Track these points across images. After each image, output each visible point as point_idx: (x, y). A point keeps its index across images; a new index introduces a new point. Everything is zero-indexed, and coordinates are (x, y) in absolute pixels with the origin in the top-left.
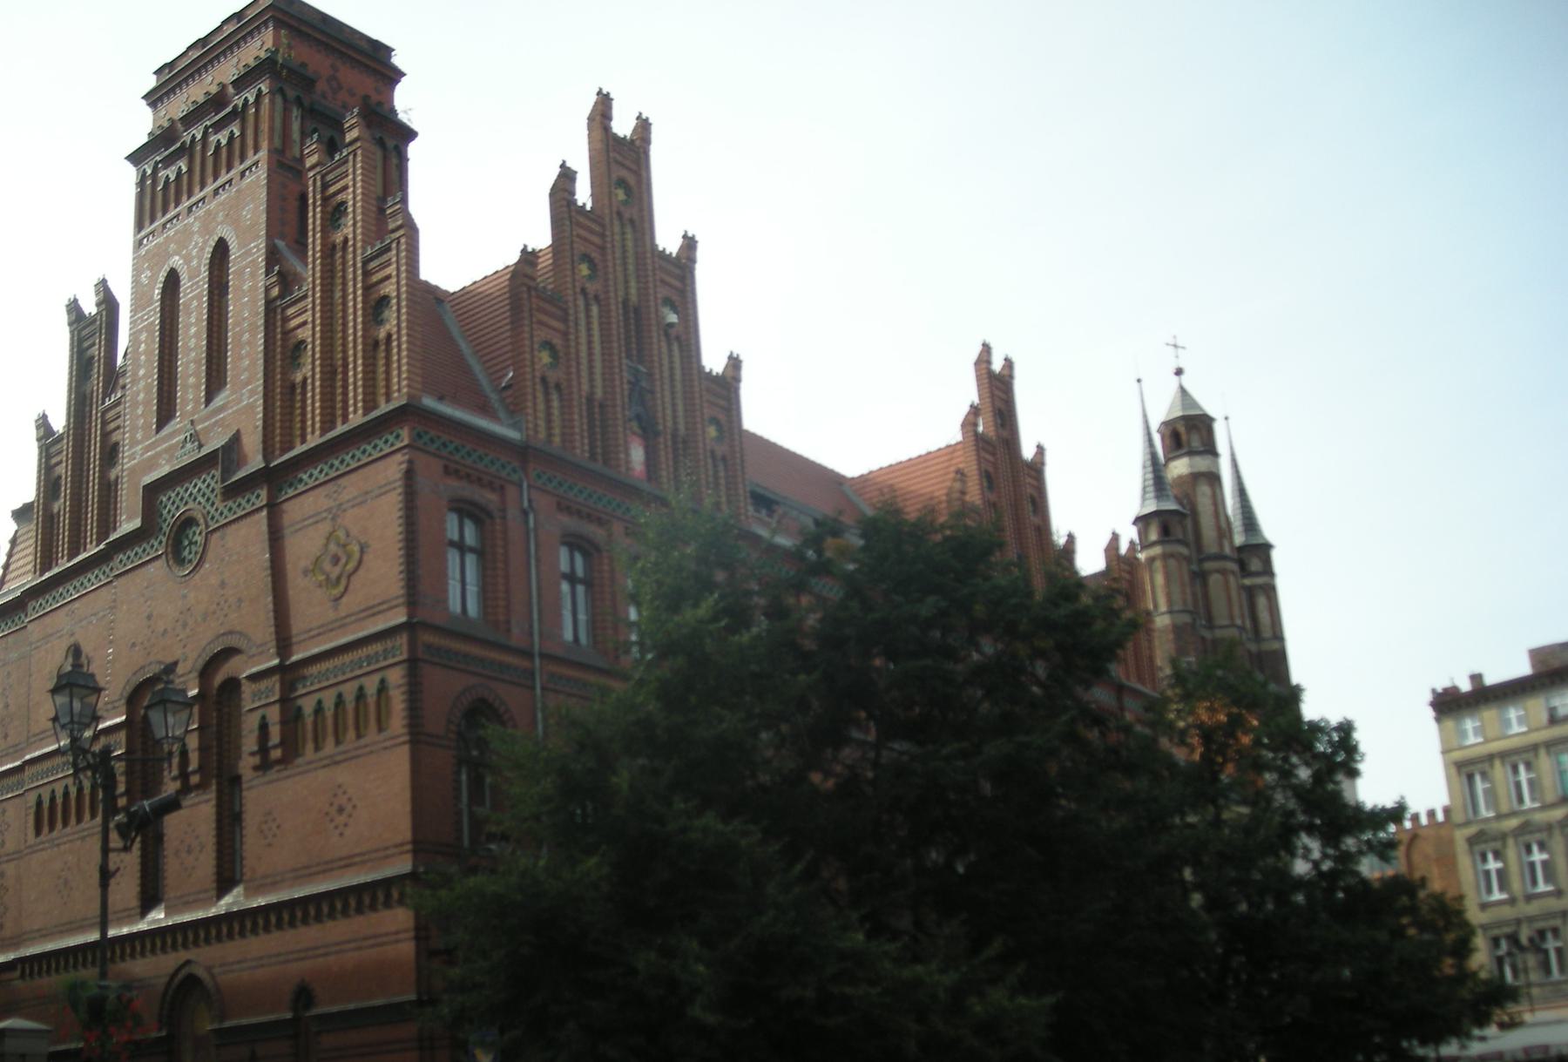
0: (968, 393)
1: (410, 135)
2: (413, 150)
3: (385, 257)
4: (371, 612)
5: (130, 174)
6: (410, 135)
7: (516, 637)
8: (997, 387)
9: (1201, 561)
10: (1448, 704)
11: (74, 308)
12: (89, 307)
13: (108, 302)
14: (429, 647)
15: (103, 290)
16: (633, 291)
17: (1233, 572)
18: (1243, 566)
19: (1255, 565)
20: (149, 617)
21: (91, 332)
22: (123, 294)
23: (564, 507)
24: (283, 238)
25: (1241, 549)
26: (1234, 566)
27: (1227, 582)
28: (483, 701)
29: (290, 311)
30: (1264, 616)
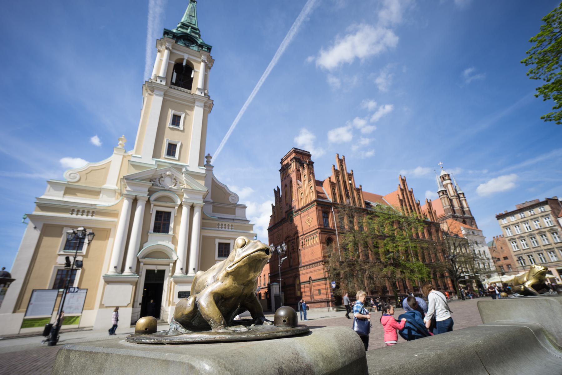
1: (313, 163)
2: (314, 165)
4: (314, 227)
6: (313, 163)
11: (274, 190)
12: (276, 190)
15: (278, 187)
21: (277, 193)
22: (280, 187)
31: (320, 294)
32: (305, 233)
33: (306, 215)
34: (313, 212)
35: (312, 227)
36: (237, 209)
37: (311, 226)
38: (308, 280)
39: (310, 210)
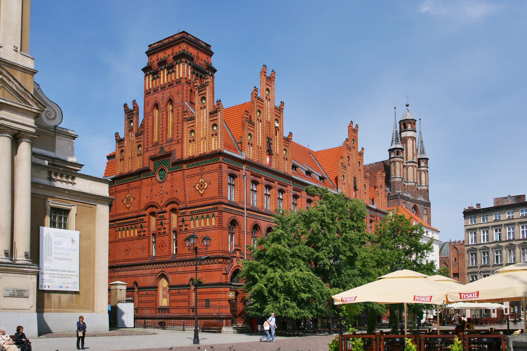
0: (345, 135)
2: (216, 75)
3: (215, 114)
4: (212, 198)
5: (143, 74)
7: (241, 205)
8: (353, 131)
9: (407, 163)
10: (469, 213)
11: (125, 106)
12: (131, 107)
13: (136, 107)
14: (224, 208)
15: (134, 102)
16: (269, 118)
17: (416, 166)
18: (419, 164)
19: (423, 164)
20: (152, 190)
23: (252, 175)
24: (187, 101)
25: (419, 159)
26: (417, 165)
27: (413, 169)
28: (234, 220)
29: (189, 122)
30: (423, 179)
31: (207, 306)
32: (189, 206)
33: (197, 175)
34: (213, 171)
35: (208, 199)
36: (57, 137)
37: (205, 196)
38: (187, 283)
39: (207, 168)
